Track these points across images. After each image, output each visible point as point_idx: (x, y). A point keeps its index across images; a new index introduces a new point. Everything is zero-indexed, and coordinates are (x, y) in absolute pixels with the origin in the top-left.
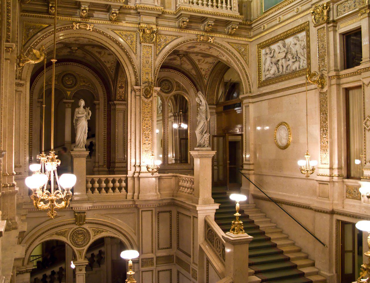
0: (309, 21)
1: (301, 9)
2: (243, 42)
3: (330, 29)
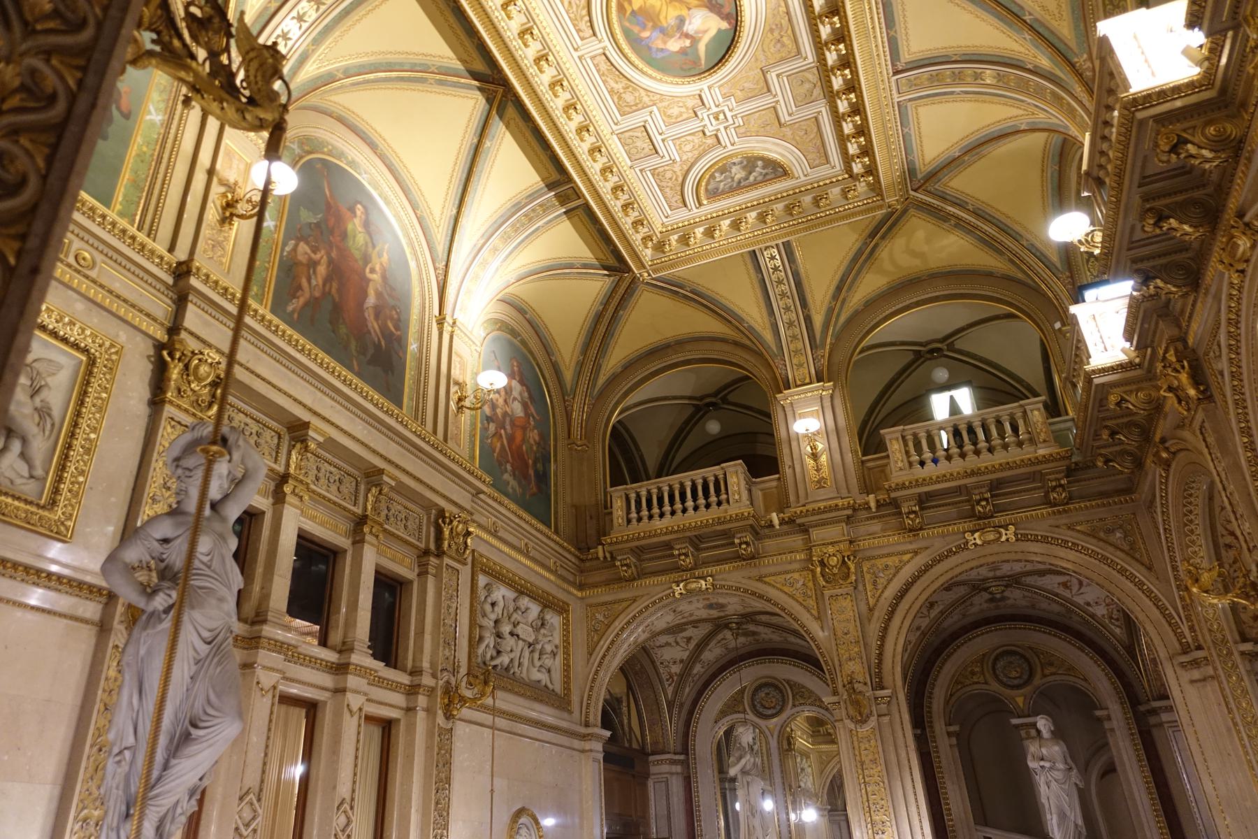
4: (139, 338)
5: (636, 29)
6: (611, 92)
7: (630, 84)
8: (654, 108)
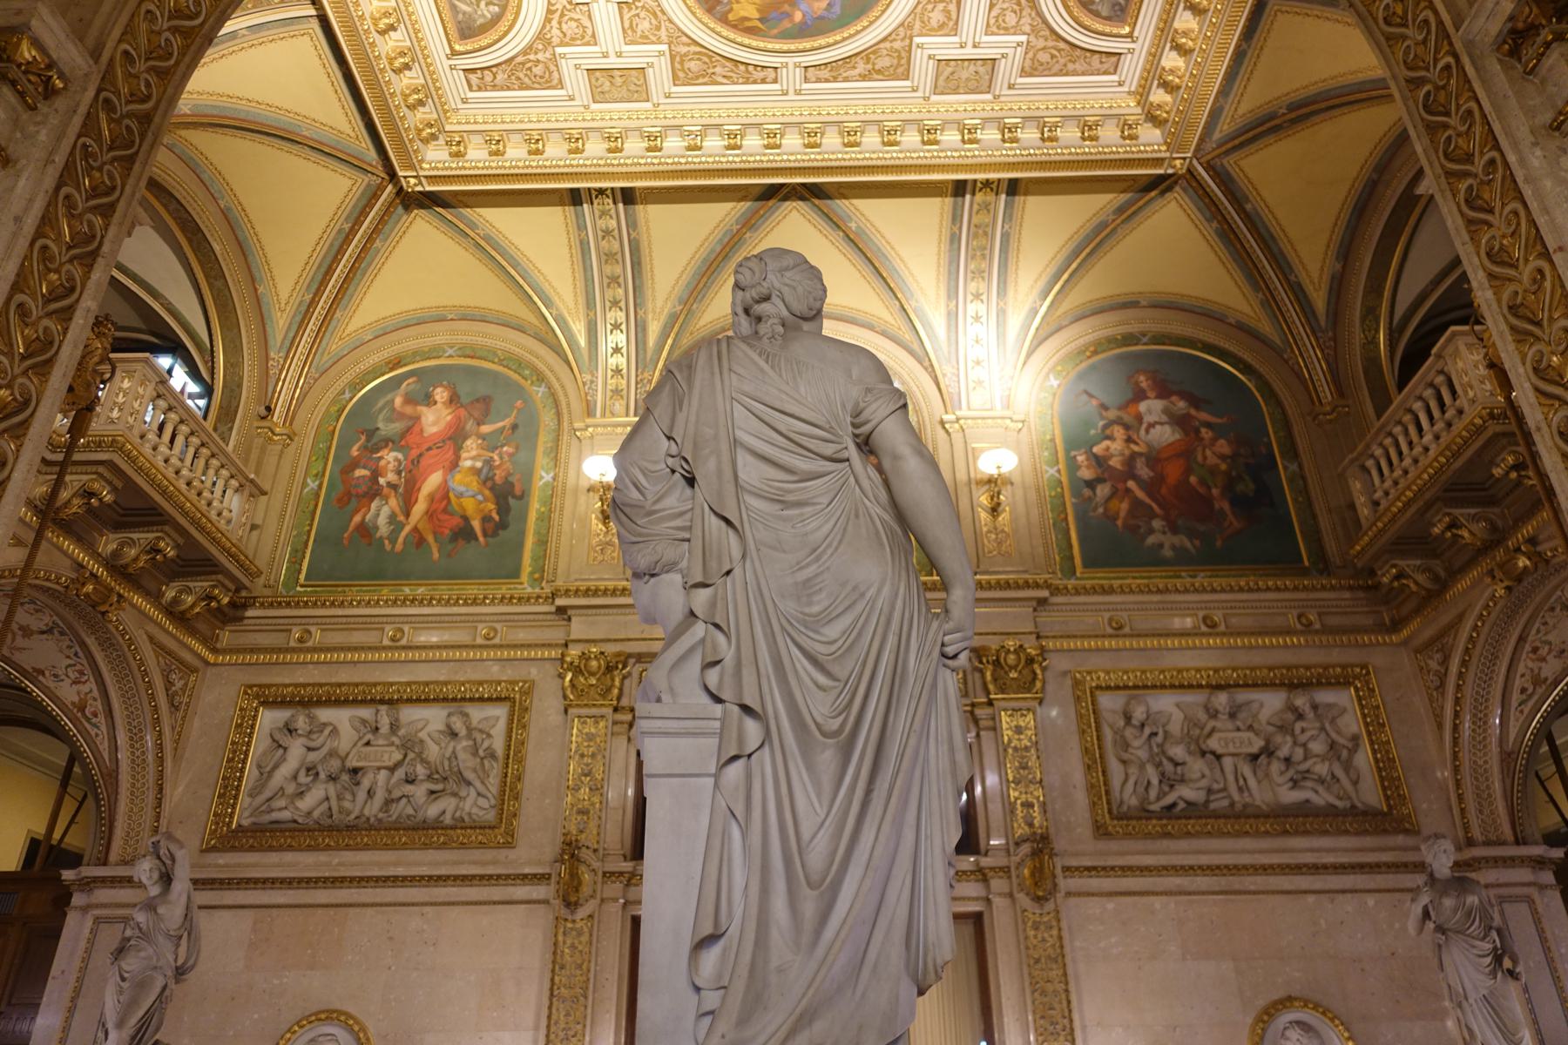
0: (533, 682)
1: (504, 634)
2: (188, 657)
3: (617, 728)
4: (548, 665)
5: (786, 24)
6: (863, 78)
7: (867, 54)
8: (917, 40)
